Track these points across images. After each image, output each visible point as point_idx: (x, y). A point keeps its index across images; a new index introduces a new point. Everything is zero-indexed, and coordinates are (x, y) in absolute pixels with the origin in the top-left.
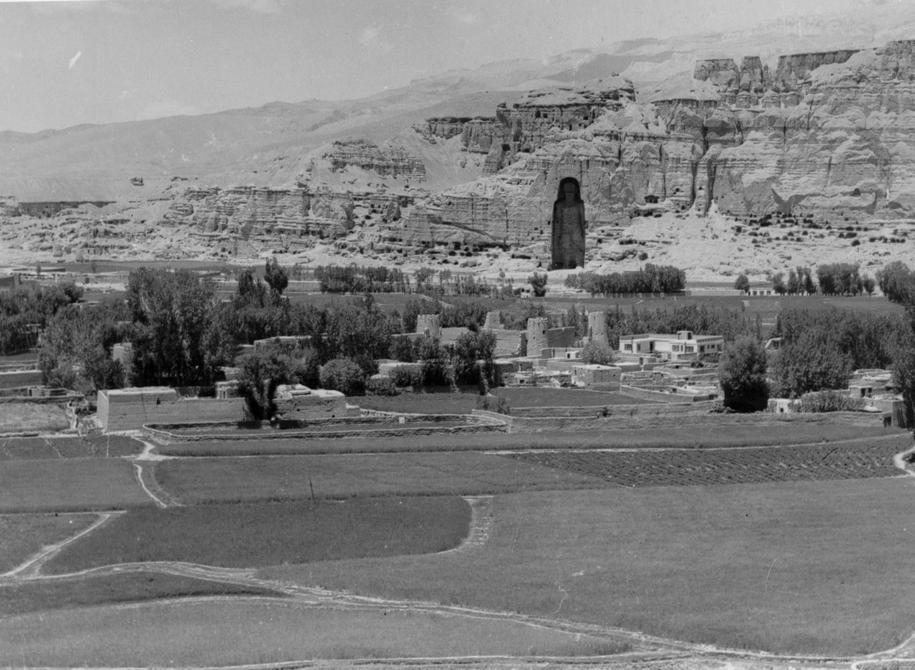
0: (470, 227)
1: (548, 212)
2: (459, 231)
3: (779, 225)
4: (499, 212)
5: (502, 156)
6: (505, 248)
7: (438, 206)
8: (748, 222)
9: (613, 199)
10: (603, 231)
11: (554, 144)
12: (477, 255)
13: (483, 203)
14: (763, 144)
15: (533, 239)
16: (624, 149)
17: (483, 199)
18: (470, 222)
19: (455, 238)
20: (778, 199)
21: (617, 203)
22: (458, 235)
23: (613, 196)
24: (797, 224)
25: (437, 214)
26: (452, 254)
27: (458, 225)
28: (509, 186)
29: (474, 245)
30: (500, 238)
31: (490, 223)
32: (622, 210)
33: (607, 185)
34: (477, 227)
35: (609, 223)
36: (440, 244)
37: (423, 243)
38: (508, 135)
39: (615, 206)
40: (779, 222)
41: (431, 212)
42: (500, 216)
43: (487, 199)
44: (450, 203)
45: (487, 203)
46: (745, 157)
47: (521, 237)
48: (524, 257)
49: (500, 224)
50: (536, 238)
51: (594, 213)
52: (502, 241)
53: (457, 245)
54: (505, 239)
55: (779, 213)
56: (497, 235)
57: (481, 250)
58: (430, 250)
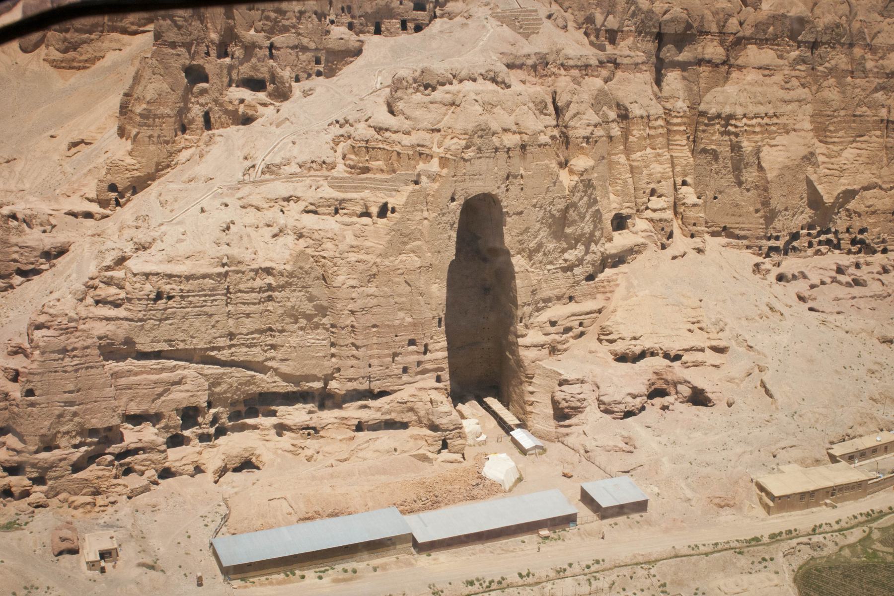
0: (223, 355)
1: (438, 291)
2: (190, 371)
3: (810, 252)
4: (309, 308)
5: (185, 99)
6: (326, 400)
7: (116, 305)
8: (765, 249)
9: (566, 237)
10: (553, 324)
11: (418, 97)
12: (243, 428)
13: (258, 283)
14: (778, 78)
15: (405, 370)
16: (568, 104)
17: (256, 271)
18: (222, 342)
19: (179, 396)
20: (815, 200)
21: (573, 247)
22: (192, 383)
23: (568, 230)
24: (838, 247)
25: (119, 331)
26: (176, 441)
27: (188, 356)
28: (310, 221)
29: (234, 404)
30: (315, 378)
31: (278, 340)
32: (580, 262)
33: (561, 204)
34: (242, 354)
35: (559, 298)
36: (136, 419)
37: (93, 432)
38: (199, 41)
39: (571, 256)
40: (810, 245)
41: (101, 328)
42: (309, 318)
43: (268, 271)
44: (159, 296)
45: (272, 283)
46: (761, 110)
47: (375, 370)
48: (390, 425)
49: (311, 337)
50: (414, 369)
51: (534, 279)
52: (317, 385)
53: (190, 415)
54: (327, 379)
55: (810, 227)
56: (306, 371)
57: (253, 413)
58: (115, 448)
